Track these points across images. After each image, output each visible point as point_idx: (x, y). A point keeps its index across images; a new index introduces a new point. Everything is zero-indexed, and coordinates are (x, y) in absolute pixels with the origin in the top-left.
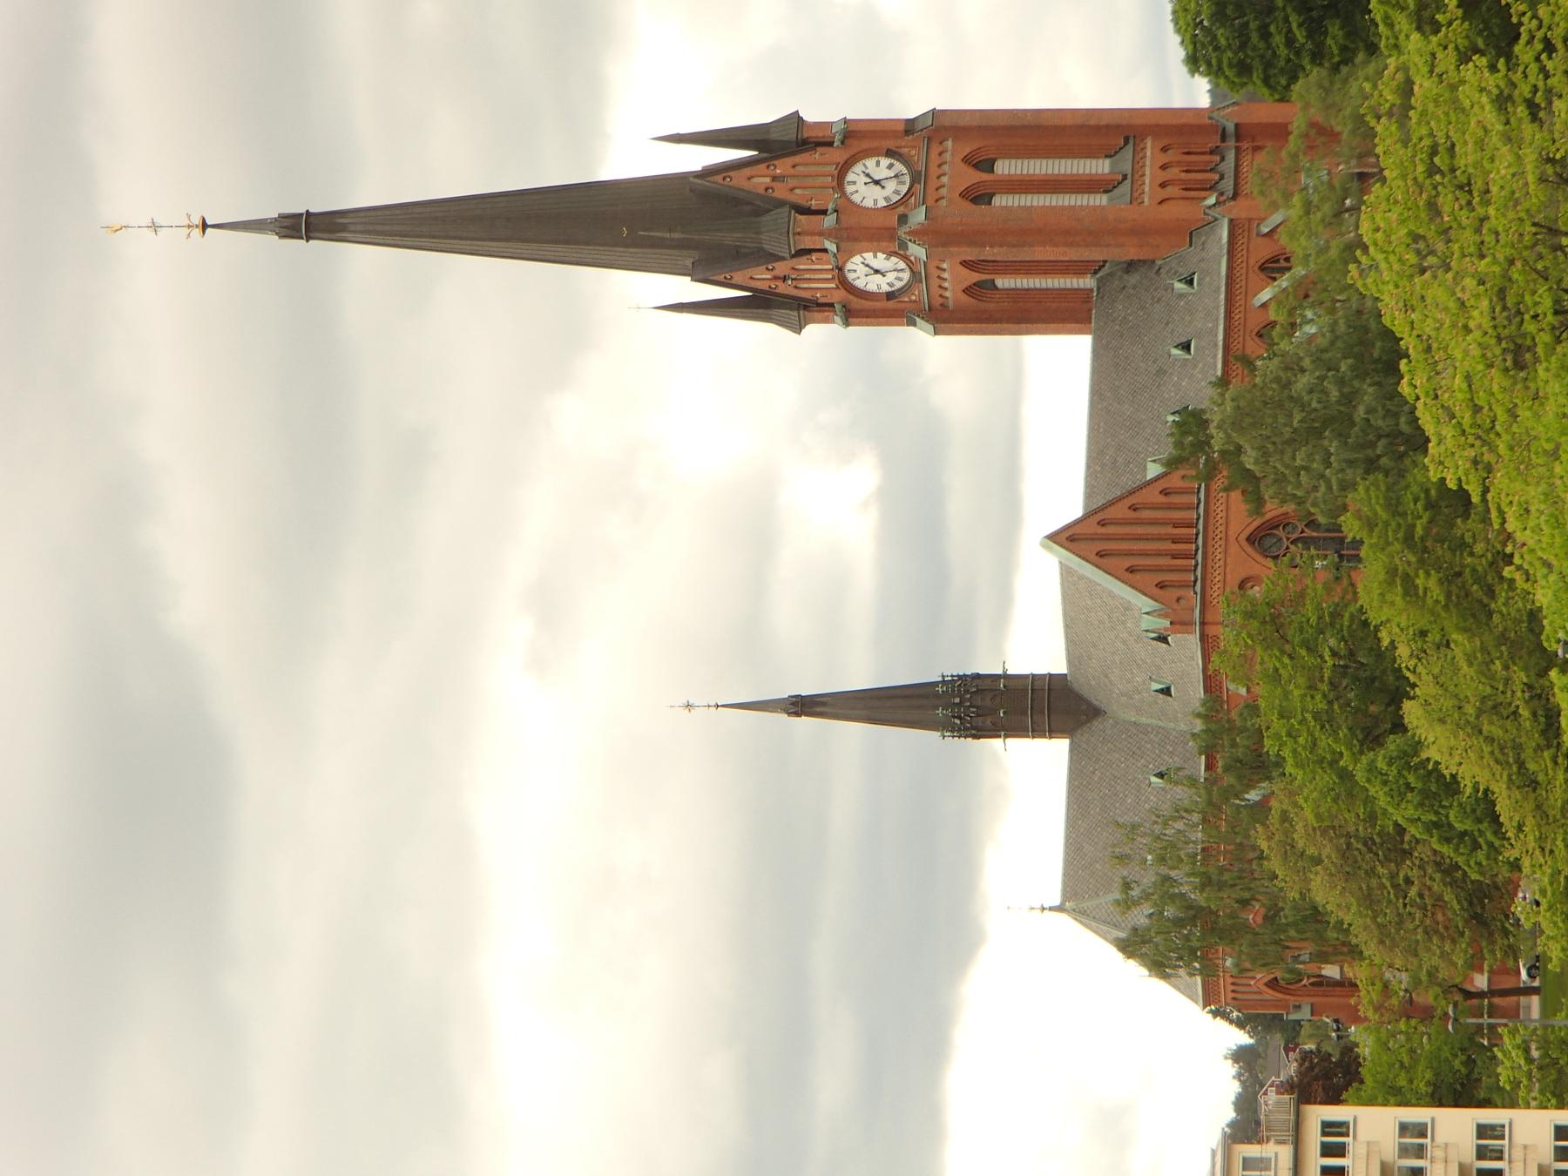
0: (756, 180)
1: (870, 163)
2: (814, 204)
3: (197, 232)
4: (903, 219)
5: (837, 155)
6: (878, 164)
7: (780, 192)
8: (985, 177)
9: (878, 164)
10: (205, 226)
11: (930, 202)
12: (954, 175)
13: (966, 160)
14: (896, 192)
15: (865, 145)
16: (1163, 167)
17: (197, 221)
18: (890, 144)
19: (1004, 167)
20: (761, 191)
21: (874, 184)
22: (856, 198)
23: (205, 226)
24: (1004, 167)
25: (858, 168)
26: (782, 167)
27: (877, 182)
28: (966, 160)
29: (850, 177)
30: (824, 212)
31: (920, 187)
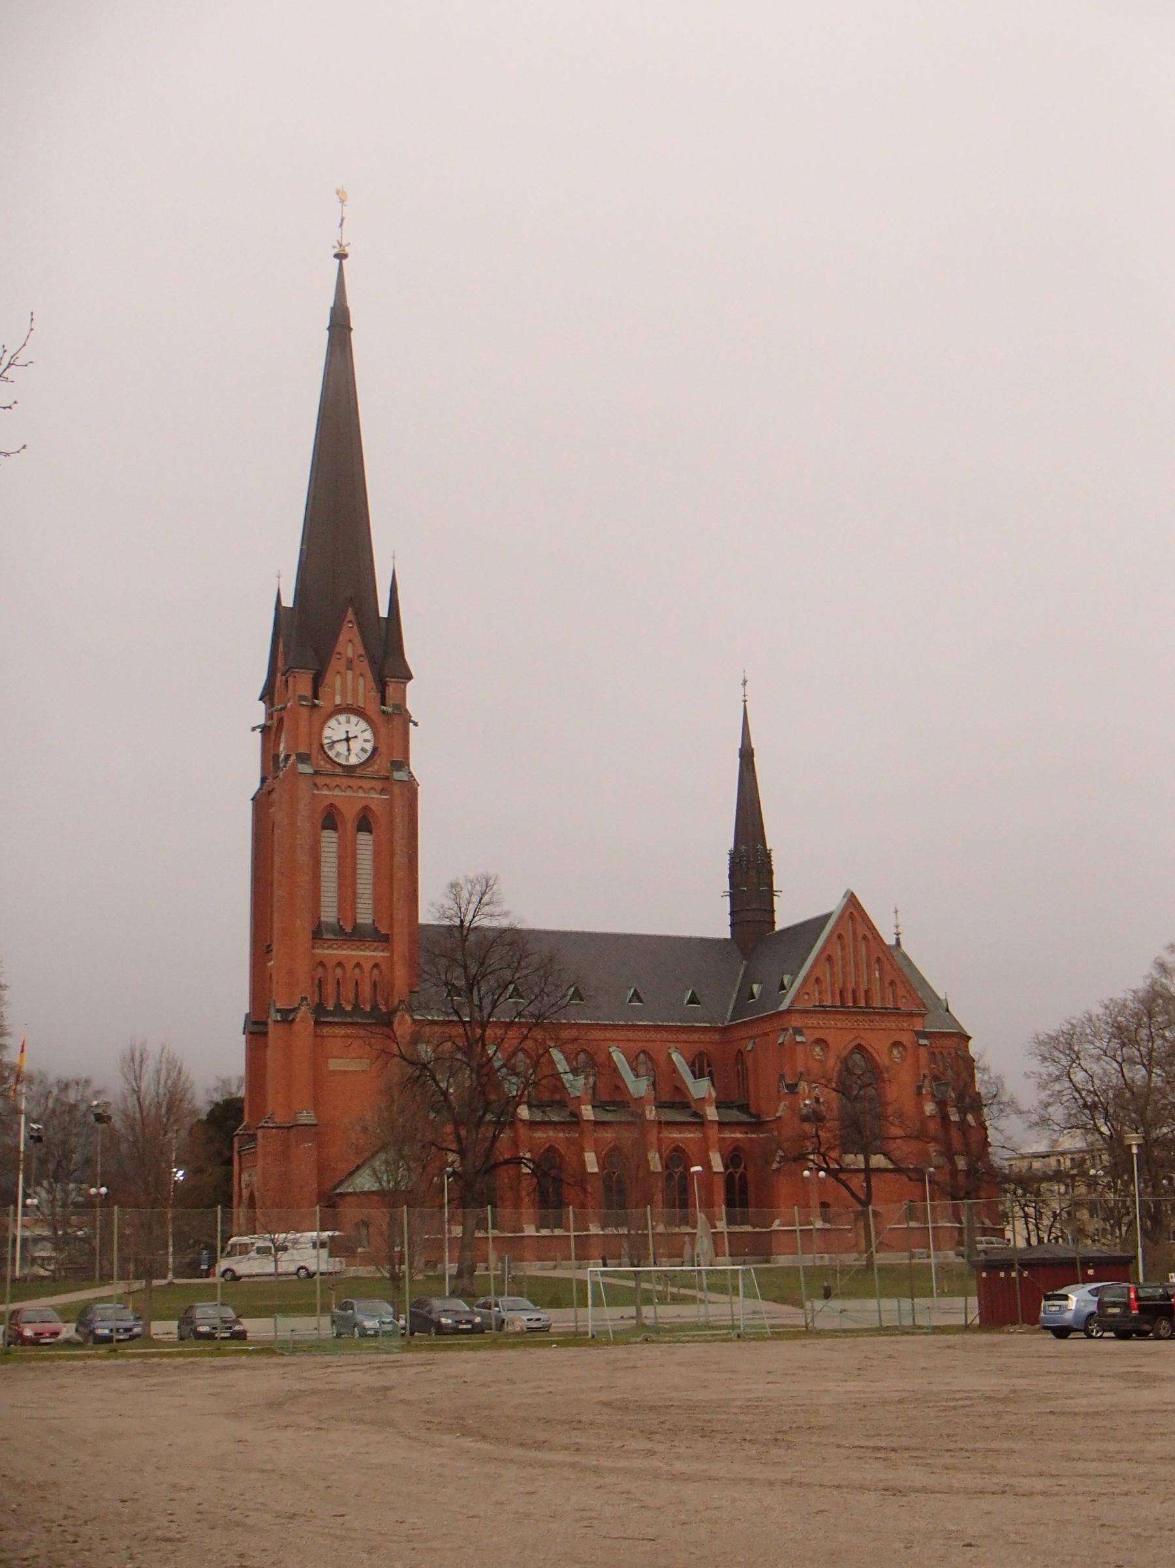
0: (350, 647)
1: (368, 735)
2: (324, 690)
3: (336, 250)
5: (372, 709)
6: (366, 741)
7: (335, 663)
8: (350, 826)
9: (366, 741)
10: (341, 256)
11: (320, 780)
12: (350, 799)
13: (366, 809)
15: (383, 731)
16: (358, 965)
18: (383, 749)
19: (364, 839)
20: (338, 649)
21: (349, 738)
22: (332, 723)
23: (341, 256)
25: (363, 725)
26: (364, 666)
27: (348, 740)
28: (366, 809)
31: (339, 770)
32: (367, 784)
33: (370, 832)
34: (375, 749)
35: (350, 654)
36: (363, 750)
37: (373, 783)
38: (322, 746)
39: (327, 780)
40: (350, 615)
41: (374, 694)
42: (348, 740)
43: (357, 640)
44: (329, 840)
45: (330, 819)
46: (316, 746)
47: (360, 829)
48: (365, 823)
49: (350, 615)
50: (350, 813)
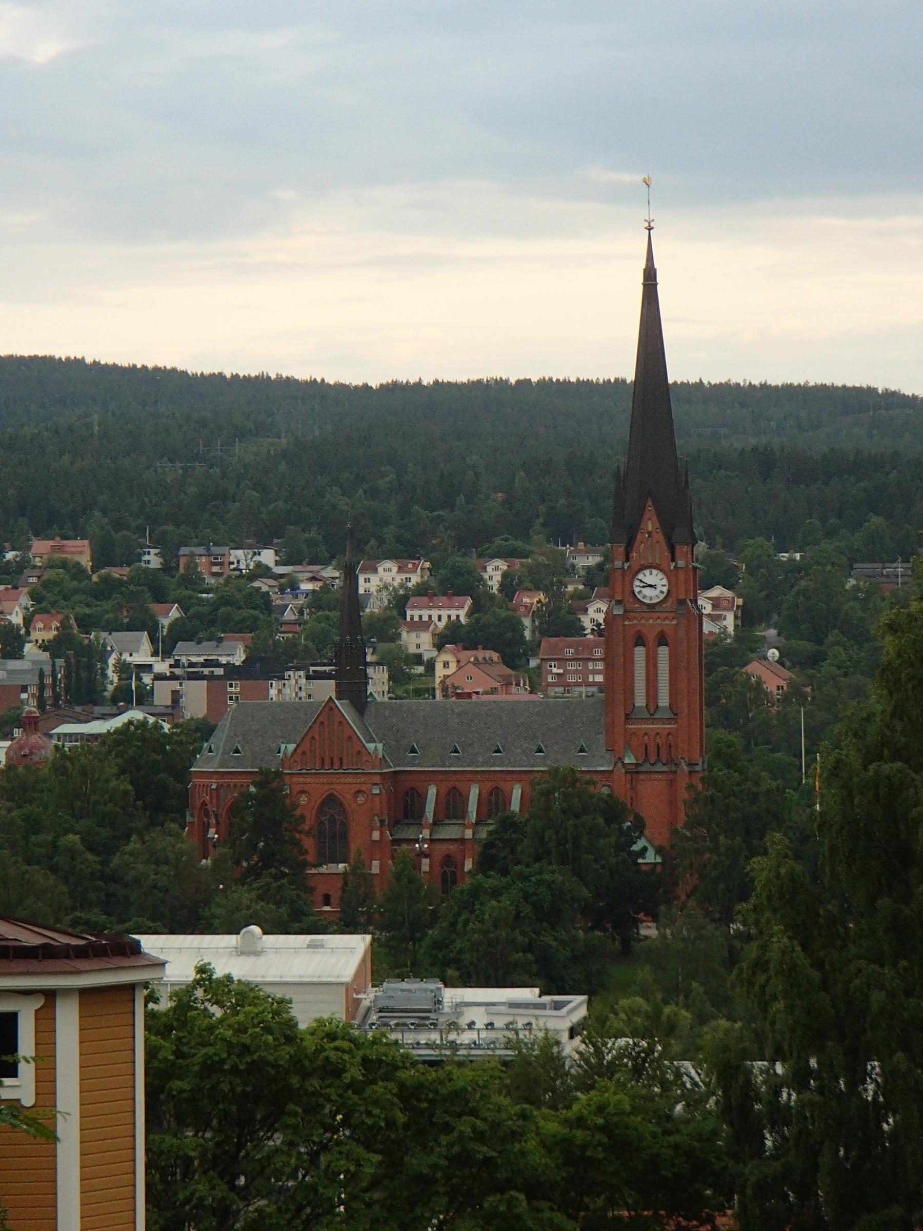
4: (619, 602)
6: (663, 586)
9: (663, 586)
10: (650, 230)
12: (651, 625)
14: (645, 597)
17: (652, 225)
19: (663, 651)
20: (642, 526)
23: (650, 230)
24: (663, 651)
25: (661, 575)
27: (651, 586)
29: (655, 572)
30: (627, 560)
31: (645, 609)
32: (663, 615)
33: (667, 645)
34: (669, 591)
35: (650, 529)
36: (662, 592)
37: (666, 615)
38: (633, 592)
39: (637, 615)
40: (649, 503)
41: (667, 554)
42: (651, 586)
43: (655, 518)
44: (640, 653)
45: (640, 640)
46: (627, 591)
47: (660, 645)
48: (662, 640)
49: (649, 503)
50: (651, 636)
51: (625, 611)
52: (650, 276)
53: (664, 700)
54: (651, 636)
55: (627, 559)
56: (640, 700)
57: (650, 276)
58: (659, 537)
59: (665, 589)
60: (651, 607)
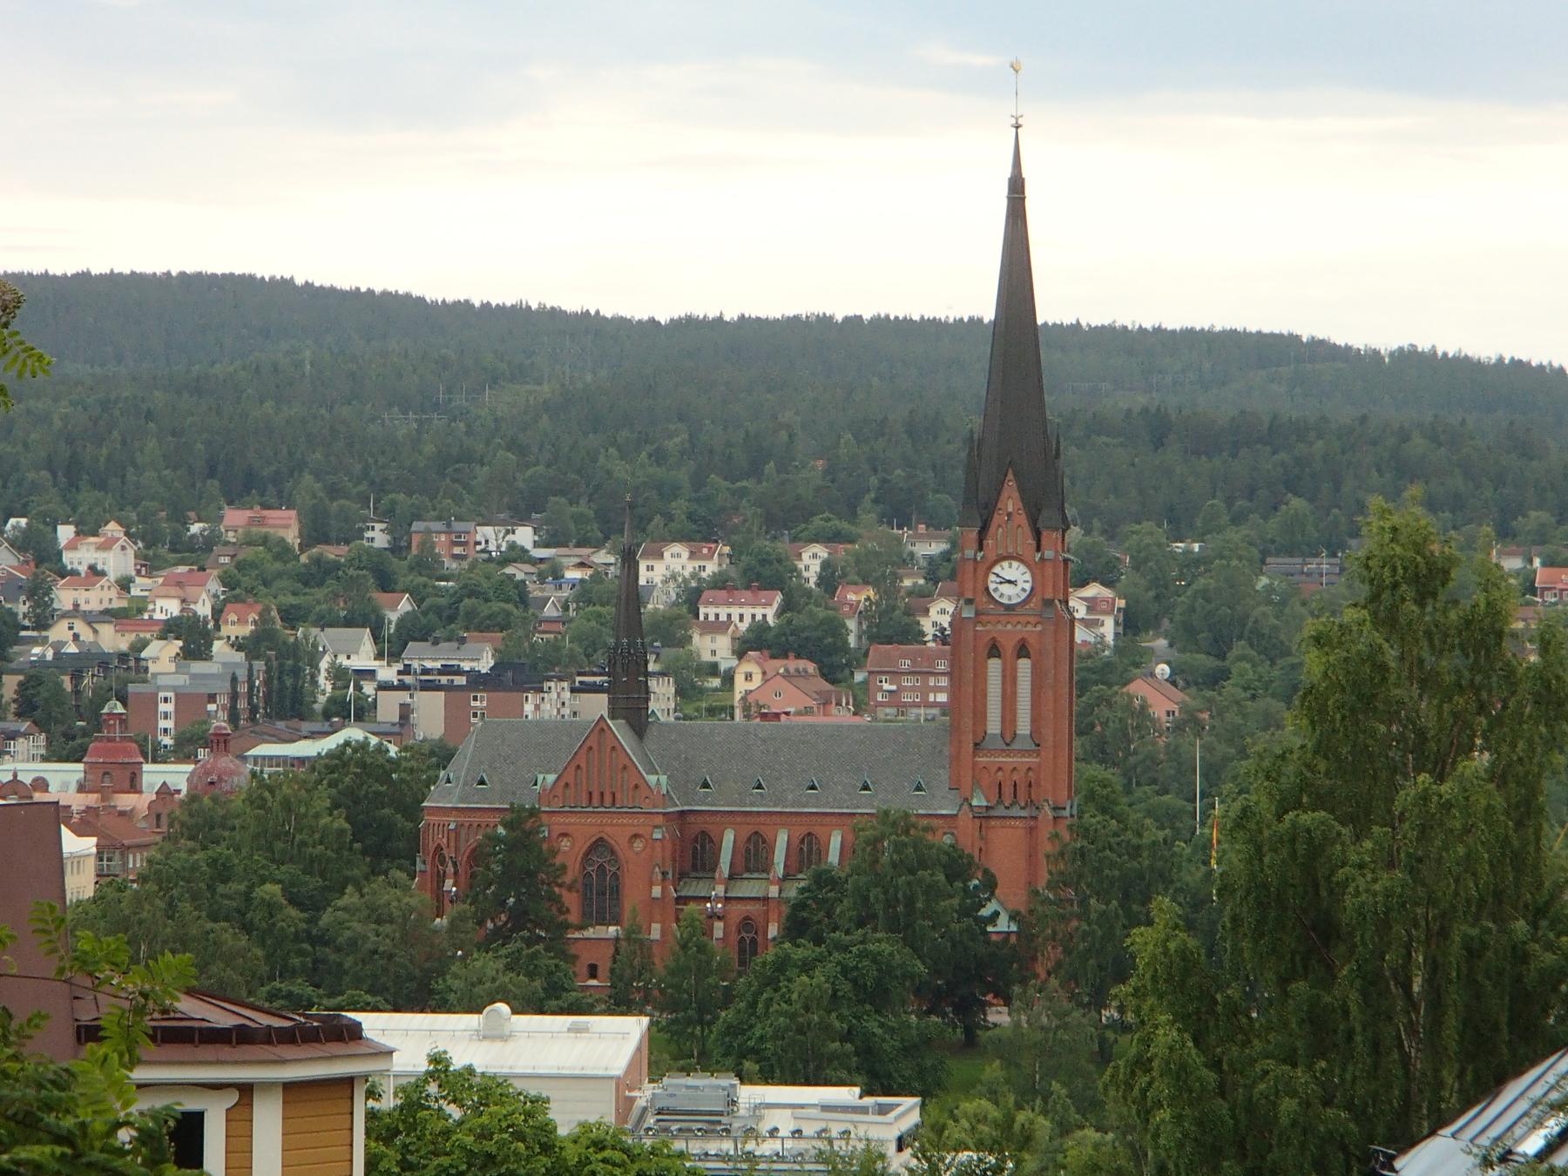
2: (989, 542)
4: (969, 602)
7: (997, 519)
10: (1017, 127)
12: (1010, 634)
14: (1002, 595)
19: (1024, 665)
25: (1023, 568)
27: (1009, 582)
29: (1015, 564)
30: (981, 548)
40: (1010, 476)
42: (1009, 582)
43: (1016, 495)
44: (994, 665)
45: (994, 651)
46: (980, 587)
48: (1023, 651)
49: (1010, 476)
50: (1009, 646)
51: (977, 613)
52: (1017, 187)
53: (1024, 727)
54: (1009, 646)
55: (981, 548)
56: (994, 726)
57: (1017, 187)
58: (1022, 518)
59: (1028, 587)
60: (1010, 608)
